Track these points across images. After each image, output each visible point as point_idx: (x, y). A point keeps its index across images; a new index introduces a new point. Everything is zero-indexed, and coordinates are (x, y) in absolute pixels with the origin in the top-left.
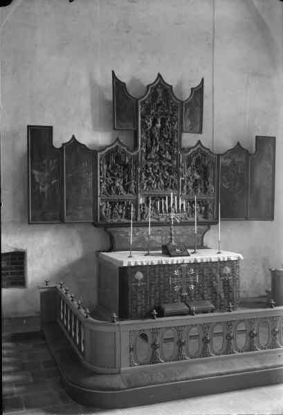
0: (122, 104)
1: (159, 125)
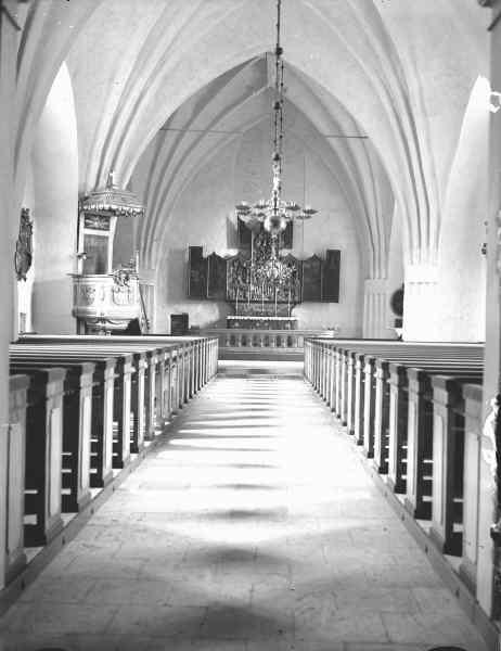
0: (244, 234)
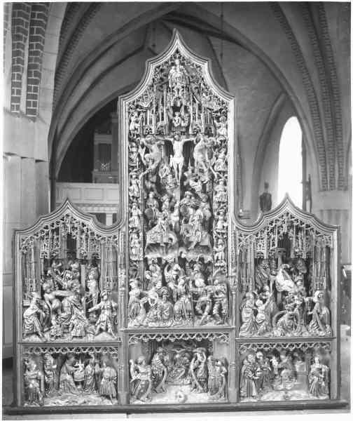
1: (178, 159)
